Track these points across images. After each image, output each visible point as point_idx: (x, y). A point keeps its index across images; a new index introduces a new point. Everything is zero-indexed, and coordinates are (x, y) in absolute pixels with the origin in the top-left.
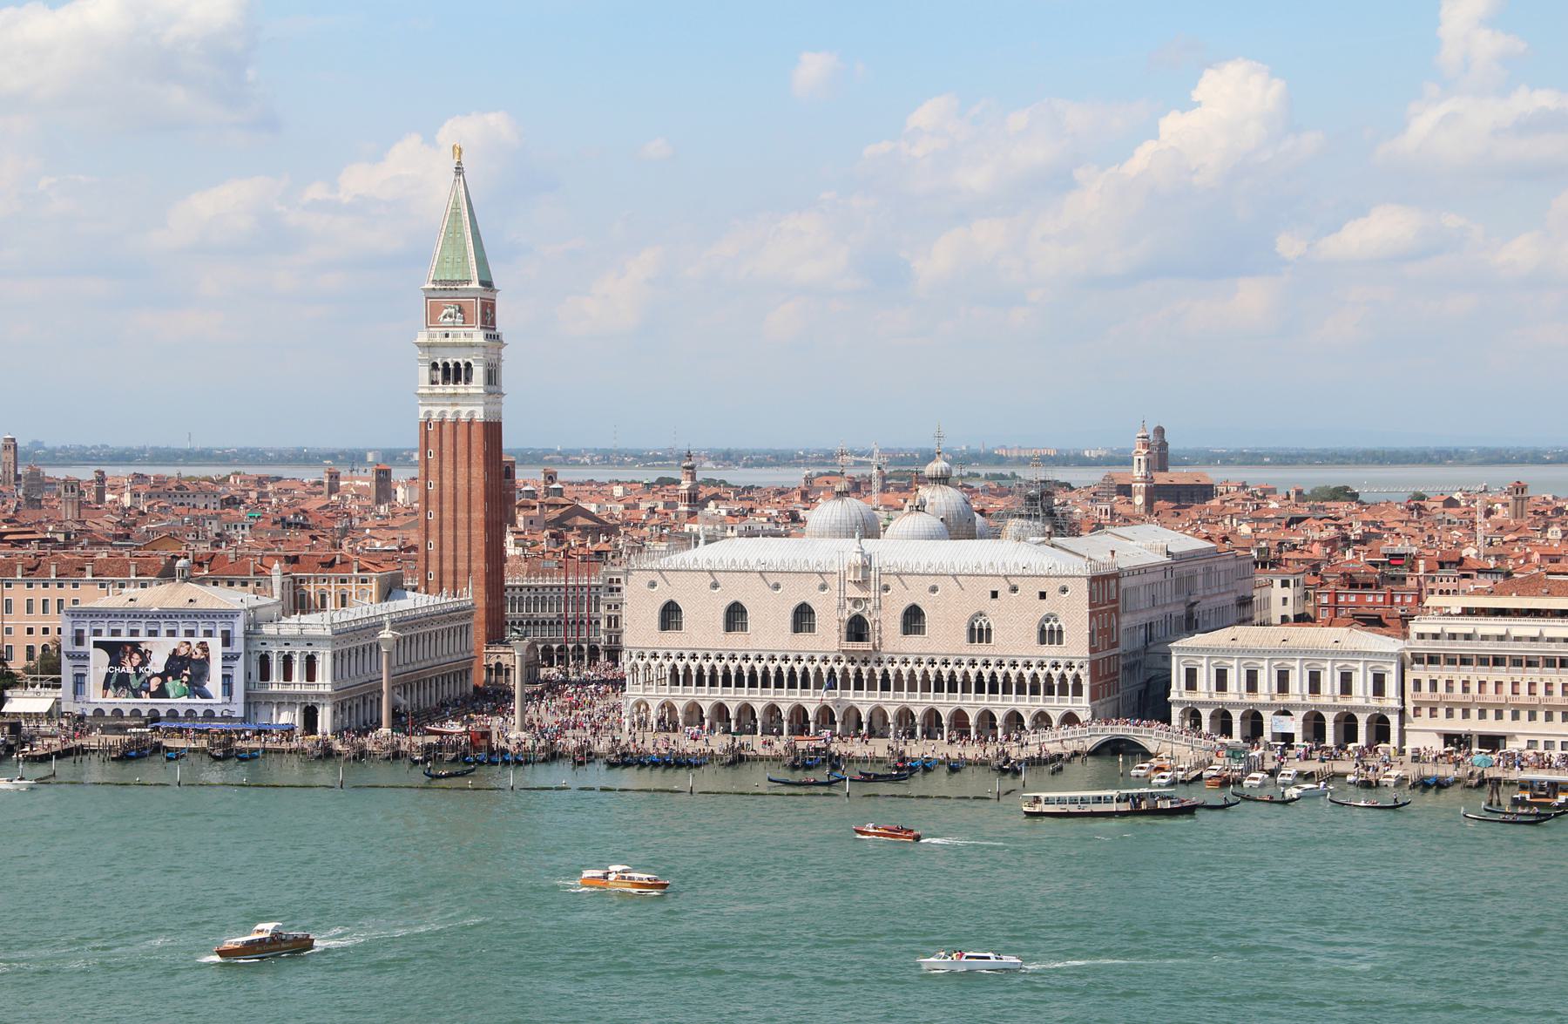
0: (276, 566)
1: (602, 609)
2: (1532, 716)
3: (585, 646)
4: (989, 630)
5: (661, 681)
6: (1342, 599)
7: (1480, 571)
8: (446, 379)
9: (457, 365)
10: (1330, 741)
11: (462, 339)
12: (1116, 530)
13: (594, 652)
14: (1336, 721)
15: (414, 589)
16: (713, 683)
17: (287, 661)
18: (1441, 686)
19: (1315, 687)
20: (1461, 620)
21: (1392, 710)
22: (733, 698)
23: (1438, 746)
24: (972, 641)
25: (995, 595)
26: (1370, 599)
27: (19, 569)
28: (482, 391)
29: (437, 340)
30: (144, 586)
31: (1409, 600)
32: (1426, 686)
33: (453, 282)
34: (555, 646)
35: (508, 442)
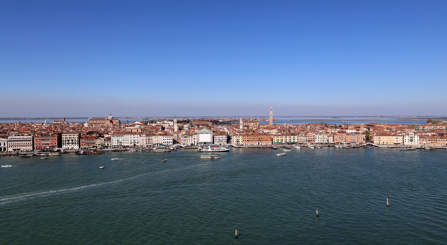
7: (16, 131)
26: (3, 135)
31: (8, 134)
32: (10, 144)
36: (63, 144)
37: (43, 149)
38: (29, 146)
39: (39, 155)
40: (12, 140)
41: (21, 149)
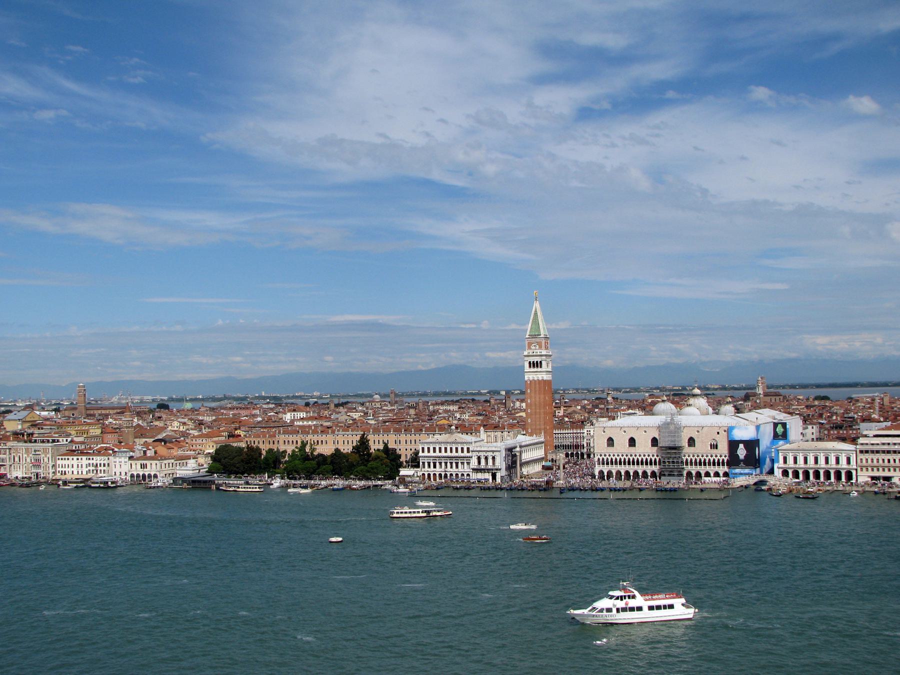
0: (482, 428)
1: (585, 440)
3: (579, 453)
5: (607, 464)
6: (832, 432)
8: (534, 366)
9: (537, 362)
11: (539, 354)
12: (757, 411)
13: (582, 454)
15: (524, 435)
16: (625, 464)
17: (486, 458)
22: (631, 469)
27: (403, 430)
28: (545, 370)
29: (531, 354)
30: (440, 435)
33: (535, 335)
34: (570, 453)
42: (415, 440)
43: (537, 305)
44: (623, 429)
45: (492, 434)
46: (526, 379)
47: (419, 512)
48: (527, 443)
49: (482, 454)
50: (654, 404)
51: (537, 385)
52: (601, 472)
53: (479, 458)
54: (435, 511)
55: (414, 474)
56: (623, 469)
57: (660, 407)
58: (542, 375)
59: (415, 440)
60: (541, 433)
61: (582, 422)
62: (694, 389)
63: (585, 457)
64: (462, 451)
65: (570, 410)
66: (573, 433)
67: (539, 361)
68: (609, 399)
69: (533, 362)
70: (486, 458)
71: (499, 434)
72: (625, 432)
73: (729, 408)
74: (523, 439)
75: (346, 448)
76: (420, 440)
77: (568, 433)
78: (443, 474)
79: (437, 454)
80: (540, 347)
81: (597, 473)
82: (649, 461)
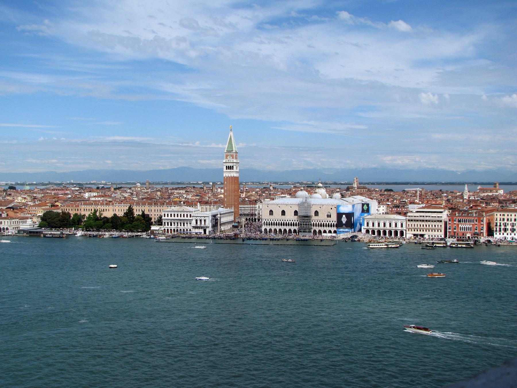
0: (199, 203)
1: (257, 211)
2: (429, 231)
4: (330, 215)
5: (269, 225)
8: (229, 169)
9: (231, 166)
10: (393, 235)
11: (232, 161)
12: (353, 197)
13: (255, 219)
14: (394, 232)
15: (222, 207)
17: (201, 221)
18: (413, 225)
19: (390, 226)
20: (417, 213)
21: (404, 230)
22: (283, 228)
23: (413, 236)
24: (327, 217)
25: (331, 209)
27: (153, 204)
32: (410, 225)
33: (230, 151)
35: (240, 181)
36: (496, 231)
37: (461, 237)
38: (438, 231)
39: (454, 246)
40: (413, 218)
41: (425, 234)
42: (160, 210)
43: (231, 134)
44: (278, 206)
45: (204, 207)
46: (224, 176)
47: (383, 245)
48: (224, 212)
49: (198, 218)
50: (296, 192)
51: (231, 180)
52: (266, 230)
53: (196, 221)
54: (391, 245)
55: (159, 229)
56: (278, 228)
57: (300, 193)
58: (233, 174)
59: (160, 210)
60: (232, 207)
61: (256, 201)
62: (318, 183)
63: (257, 221)
64: (187, 216)
65: (249, 194)
66: (250, 207)
67: (232, 165)
68: (271, 188)
69: (229, 166)
70: (201, 221)
71: (208, 207)
72: (279, 207)
73: (338, 195)
74: (222, 210)
75: (120, 214)
76: (163, 210)
77: (247, 207)
78: (176, 229)
79: (173, 218)
80: (233, 158)
81: (263, 230)
82: (292, 224)
